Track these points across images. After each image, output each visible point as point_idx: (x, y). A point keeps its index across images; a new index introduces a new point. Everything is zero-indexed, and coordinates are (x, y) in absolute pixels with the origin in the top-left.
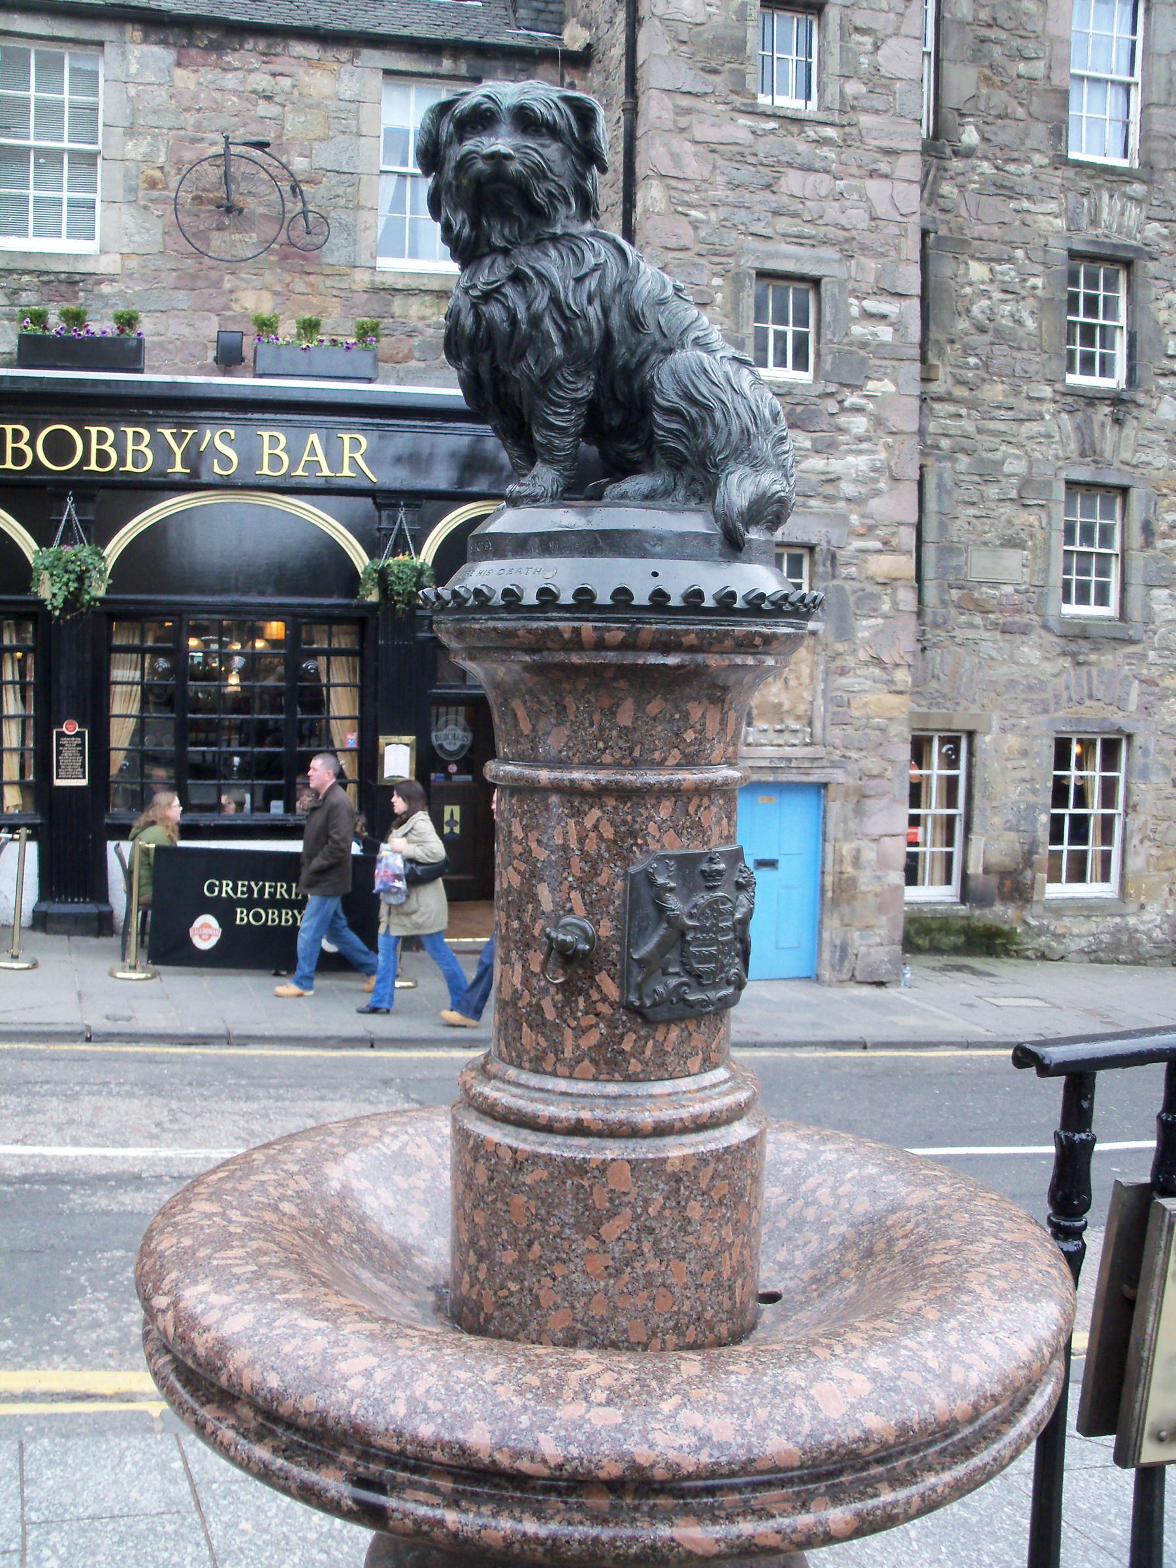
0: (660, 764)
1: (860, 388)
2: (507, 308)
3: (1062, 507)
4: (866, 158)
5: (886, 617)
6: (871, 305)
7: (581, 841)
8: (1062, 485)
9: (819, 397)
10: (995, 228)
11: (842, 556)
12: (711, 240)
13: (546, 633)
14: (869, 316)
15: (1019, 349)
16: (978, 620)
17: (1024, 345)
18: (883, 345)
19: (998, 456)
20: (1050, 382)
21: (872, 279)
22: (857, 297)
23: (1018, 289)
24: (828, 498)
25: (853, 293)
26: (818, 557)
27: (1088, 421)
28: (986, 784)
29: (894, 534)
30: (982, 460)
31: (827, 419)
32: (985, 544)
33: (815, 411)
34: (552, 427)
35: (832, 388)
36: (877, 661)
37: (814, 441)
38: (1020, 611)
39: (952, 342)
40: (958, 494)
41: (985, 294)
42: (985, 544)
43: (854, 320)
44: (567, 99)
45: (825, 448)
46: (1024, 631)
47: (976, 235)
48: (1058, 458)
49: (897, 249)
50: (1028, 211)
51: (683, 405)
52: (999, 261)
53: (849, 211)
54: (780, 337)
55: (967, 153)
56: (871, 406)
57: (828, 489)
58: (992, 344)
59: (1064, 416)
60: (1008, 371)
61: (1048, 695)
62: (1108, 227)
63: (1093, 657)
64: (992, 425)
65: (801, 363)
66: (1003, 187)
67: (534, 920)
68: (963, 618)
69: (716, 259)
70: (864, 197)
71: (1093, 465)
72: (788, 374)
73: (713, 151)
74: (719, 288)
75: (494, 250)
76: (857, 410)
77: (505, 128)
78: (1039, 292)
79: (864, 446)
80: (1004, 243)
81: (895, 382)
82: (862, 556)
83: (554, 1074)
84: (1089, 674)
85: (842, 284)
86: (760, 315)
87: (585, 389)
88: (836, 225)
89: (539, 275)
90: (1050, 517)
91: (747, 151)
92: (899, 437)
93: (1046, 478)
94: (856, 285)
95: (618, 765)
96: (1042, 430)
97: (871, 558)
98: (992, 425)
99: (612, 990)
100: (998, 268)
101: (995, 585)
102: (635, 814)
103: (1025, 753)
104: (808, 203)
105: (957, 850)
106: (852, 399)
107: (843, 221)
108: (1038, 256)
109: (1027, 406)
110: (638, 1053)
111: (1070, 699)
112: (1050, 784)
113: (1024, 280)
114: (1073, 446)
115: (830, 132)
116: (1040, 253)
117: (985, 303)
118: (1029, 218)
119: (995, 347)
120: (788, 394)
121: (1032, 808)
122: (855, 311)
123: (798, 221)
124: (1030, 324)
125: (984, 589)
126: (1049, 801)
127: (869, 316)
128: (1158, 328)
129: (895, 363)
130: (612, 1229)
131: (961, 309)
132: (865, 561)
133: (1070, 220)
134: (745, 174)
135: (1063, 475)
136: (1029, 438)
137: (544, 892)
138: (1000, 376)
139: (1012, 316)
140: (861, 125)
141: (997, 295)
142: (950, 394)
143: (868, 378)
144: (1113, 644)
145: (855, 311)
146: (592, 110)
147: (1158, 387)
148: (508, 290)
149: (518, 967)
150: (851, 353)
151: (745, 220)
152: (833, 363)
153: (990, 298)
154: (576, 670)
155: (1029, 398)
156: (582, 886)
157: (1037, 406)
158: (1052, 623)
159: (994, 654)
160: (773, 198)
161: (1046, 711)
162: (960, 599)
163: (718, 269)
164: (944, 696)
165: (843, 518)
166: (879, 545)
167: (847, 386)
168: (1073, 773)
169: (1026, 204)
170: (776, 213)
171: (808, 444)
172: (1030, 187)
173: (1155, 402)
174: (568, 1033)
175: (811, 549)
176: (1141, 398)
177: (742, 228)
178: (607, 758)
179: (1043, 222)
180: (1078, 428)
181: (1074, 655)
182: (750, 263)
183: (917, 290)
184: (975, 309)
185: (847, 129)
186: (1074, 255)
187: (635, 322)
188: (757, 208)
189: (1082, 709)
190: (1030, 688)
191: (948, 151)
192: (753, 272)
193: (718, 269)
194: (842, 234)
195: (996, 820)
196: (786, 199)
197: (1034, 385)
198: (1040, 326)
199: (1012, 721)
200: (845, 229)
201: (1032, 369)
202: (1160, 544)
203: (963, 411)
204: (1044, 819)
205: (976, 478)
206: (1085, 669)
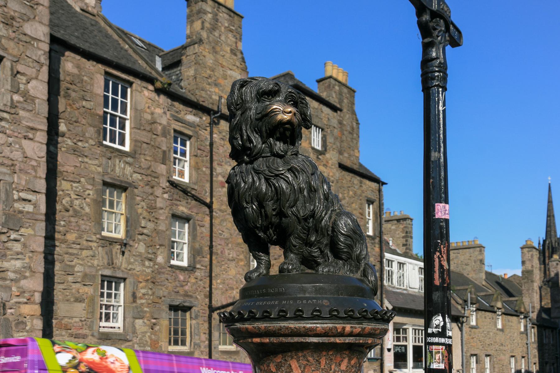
1: (18, 231)
5: (27, 331)
17: (85, 218)
19: (73, 263)
22: (17, 191)
27: (111, 251)
32: (68, 300)
35: (5, 230)
42: (68, 300)
53: (14, 152)
59: (100, 248)
64: (70, 251)
76: (16, 240)
82: (17, 305)
97: (22, 306)
106: (13, 236)
109: (85, 242)
122: (16, 197)
124: (87, 210)
128: (138, 215)
132: (19, 307)
135: (100, 273)
144: (121, 342)
145: (16, 197)
147: (138, 239)
152: (5, 219)
155: (87, 240)
157: (90, 244)
158: (96, 334)
167: (11, 230)
173: (137, 245)
176: (131, 243)
186: (106, 184)
202: (139, 301)
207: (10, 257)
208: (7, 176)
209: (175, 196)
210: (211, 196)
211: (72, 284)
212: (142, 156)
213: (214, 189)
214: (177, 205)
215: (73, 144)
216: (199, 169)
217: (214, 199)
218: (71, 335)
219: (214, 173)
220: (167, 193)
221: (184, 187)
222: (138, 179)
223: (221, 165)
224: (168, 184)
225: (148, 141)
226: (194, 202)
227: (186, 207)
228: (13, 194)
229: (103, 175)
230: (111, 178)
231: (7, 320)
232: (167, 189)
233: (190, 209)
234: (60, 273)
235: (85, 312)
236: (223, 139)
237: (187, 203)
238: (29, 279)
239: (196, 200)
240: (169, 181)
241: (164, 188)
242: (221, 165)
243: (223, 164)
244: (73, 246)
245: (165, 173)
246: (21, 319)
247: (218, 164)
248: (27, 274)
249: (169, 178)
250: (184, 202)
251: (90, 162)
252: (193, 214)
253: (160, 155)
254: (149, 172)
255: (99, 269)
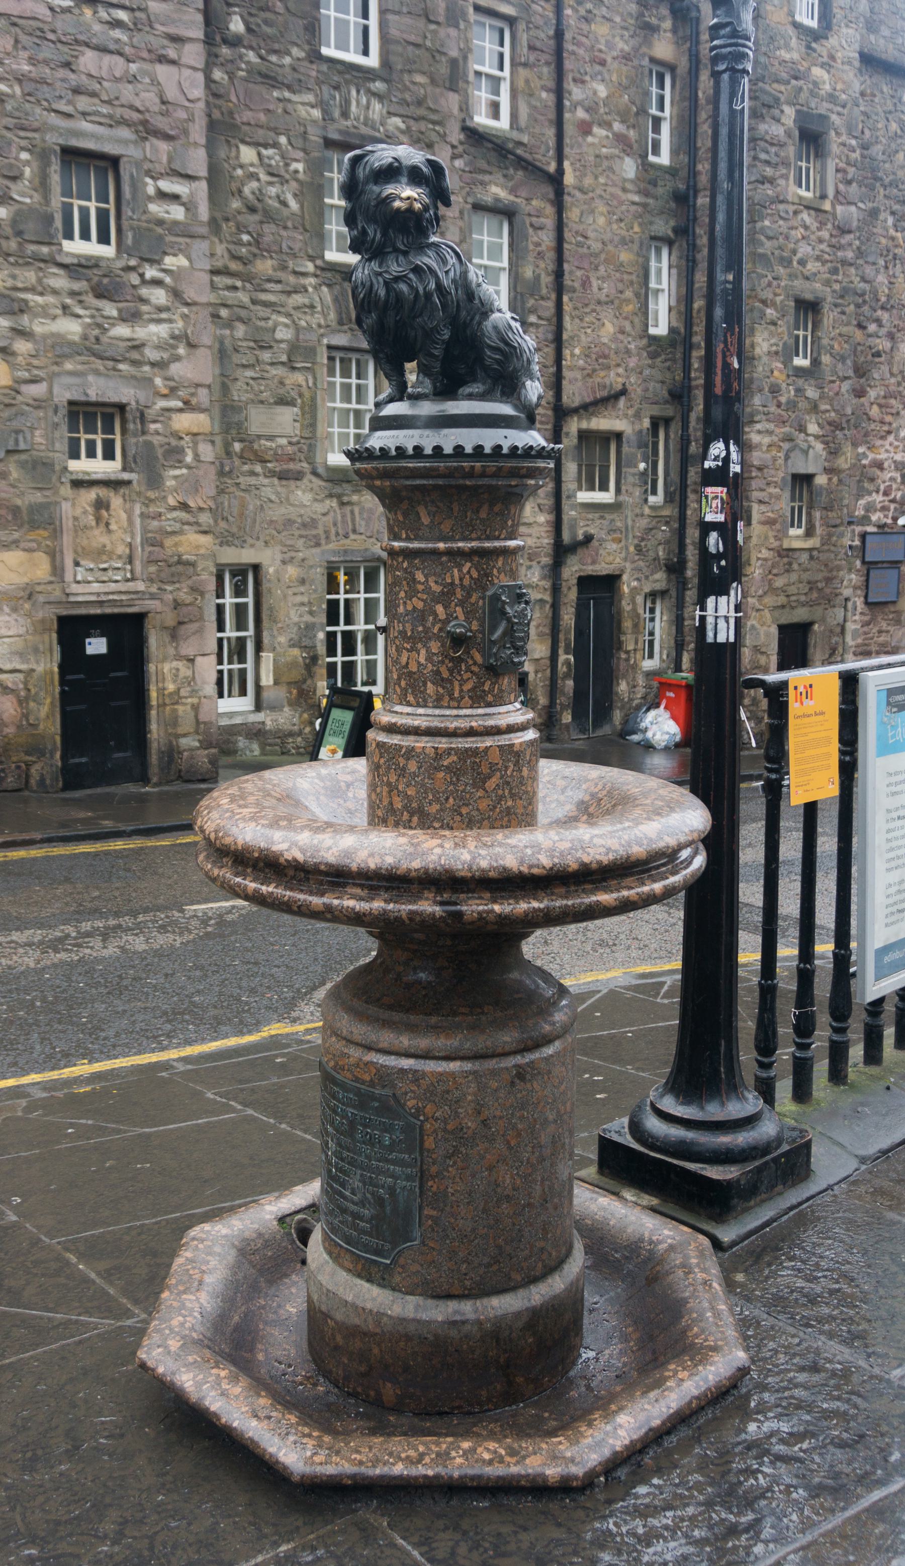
0: (498, 538)
2: (411, 287)
3: (325, 370)
4: (157, 42)
5: (189, 467)
6: (166, 185)
7: (461, 579)
8: (325, 349)
9: (123, 269)
10: (262, 117)
11: (150, 413)
12: (17, 114)
13: (456, 468)
14: (163, 195)
15: (285, 228)
16: (258, 468)
17: (289, 224)
18: (176, 223)
20: (312, 258)
21: (165, 159)
22: (152, 178)
23: (283, 173)
24: (135, 363)
25: (149, 173)
26: (129, 416)
28: (271, 609)
29: (192, 395)
30: (258, 329)
31: (132, 291)
33: (118, 283)
34: (432, 355)
35: (133, 262)
36: (184, 506)
37: (120, 311)
38: (292, 460)
39: (227, 220)
40: (237, 359)
41: (254, 176)
42: (262, 402)
43: (150, 199)
44: (428, 161)
45: (131, 317)
46: (298, 476)
47: (245, 120)
48: (320, 326)
49: (186, 132)
50: (289, 101)
51: (502, 345)
52: (266, 146)
54: (84, 212)
55: (234, 42)
56: (168, 280)
57: (135, 355)
58: (262, 222)
59: (325, 289)
60: (275, 248)
61: (320, 531)
62: (357, 119)
63: (355, 498)
64: (263, 297)
65: (104, 239)
66: (266, 76)
67: (433, 625)
68: (246, 468)
69: (22, 134)
70: (155, 82)
71: (349, 334)
72: (92, 248)
73: (14, 24)
74: (27, 163)
75: (396, 250)
76: (157, 283)
77: (404, 180)
78: (301, 176)
79: (164, 316)
80: (269, 129)
81: (189, 259)
82: (167, 414)
83: (449, 707)
84: (352, 512)
85: (138, 164)
86: (67, 193)
87: (446, 334)
88: (132, 107)
89: (429, 268)
90: (315, 378)
91: (46, 28)
92: (194, 308)
93: (310, 344)
94: (151, 166)
95: (479, 539)
96: (306, 301)
97: (176, 417)
98: (263, 297)
99: (478, 658)
100: (264, 152)
101: (271, 438)
102: (488, 564)
103: (303, 582)
104: (105, 84)
105: (249, 665)
106: (151, 273)
107: (138, 104)
108: (299, 143)
109: (292, 279)
110: (491, 691)
111: (337, 534)
112: (324, 606)
113: (287, 165)
114: (332, 316)
115: (122, 15)
116: (300, 141)
117: (254, 184)
118: (289, 107)
119: (265, 226)
120: (97, 266)
121: (310, 628)
122: (151, 190)
123: (96, 101)
124: (294, 205)
125: (263, 442)
126: (324, 620)
127: (163, 195)
129: (188, 240)
130: (491, 784)
131: (234, 189)
132: (170, 419)
133: (325, 112)
134: (47, 52)
135: (325, 341)
136: (296, 308)
137: (440, 609)
138: (269, 251)
139: (278, 197)
140: (151, 10)
141: (263, 177)
142: (226, 267)
143: (165, 253)
146: (442, 169)
148: (411, 276)
149: (423, 652)
150: (149, 230)
151: (47, 96)
152: (134, 237)
153: (258, 180)
154: (465, 488)
155: (295, 273)
156: (461, 603)
158: (320, 470)
159: (273, 497)
160: (72, 76)
161: (318, 545)
162: (242, 450)
163: (24, 143)
164: (233, 535)
165: (150, 380)
166: (180, 404)
168: (342, 597)
169: (287, 94)
170: (77, 91)
171: (115, 313)
172: (290, 77)
174: (456, 684)
175: (121, 408)
177: (45, 103)
178: (474, 535)
179: (302, 111)
180: (336, 300)
181: (339, 497)
182: (53, 140)
183: (203, 172)
184: (247, 190)
185: (138, 14)
186: (329, 143)
187: (470, 295)
188: (59, 84)
189: (347, 542)
190: (304, 525)
191: (218, 38)
192: (58, 148)
193: (24, 143)
194: (136, 116)
195: (282, 639)
196: (84, 77)
197: (299, 261)
198: (302, 207)
199: (293, 554)
200: (138, 111)
201: (297, 246)
203: (239, 284)
204: (321, 636)
205: (252, 344)
206: (348, 509)
207: (146, 317)
208: (132, 146)
209: (482, 164)
210: (560, 157)
211: (268, 368)
212: (406, 77)
213: (567, 141)
214: (482, 183)
215: (258, 60)
216: (531, 95)
217: (566, 164)
218: (272, 474)
219: (567, 103)
220: (461, 156)
221: (499, 142)
222: (398, 128)
223: (583, 82)
224: (462, 137)
225: (419, 41)
226: (520, 173)
227: (503, 187)
228: (146, 184)
229: (325, 128)
230: (340, 132)
231: (149, 445)
232: (460, 149)
233: (513, 191)
234: (244, 344)
235: (297, 425)
236: (586, 20)
237: (505, 176)
238: (185, 361)
239: (525, 169)
240: (465, 129)
241: (453, 147)
242: (583, 82)
243: (587, 78)
244: (269, 286)
245: (456, 111)
246: (174, 442)
247: (574, 80)
248: (181, 351)
249: (464, 120)
250: (498, 177)
251: (295, 98)
252: (518, 200)
253: (444, 70)
254: (421, 112)
255: (322, 335)
